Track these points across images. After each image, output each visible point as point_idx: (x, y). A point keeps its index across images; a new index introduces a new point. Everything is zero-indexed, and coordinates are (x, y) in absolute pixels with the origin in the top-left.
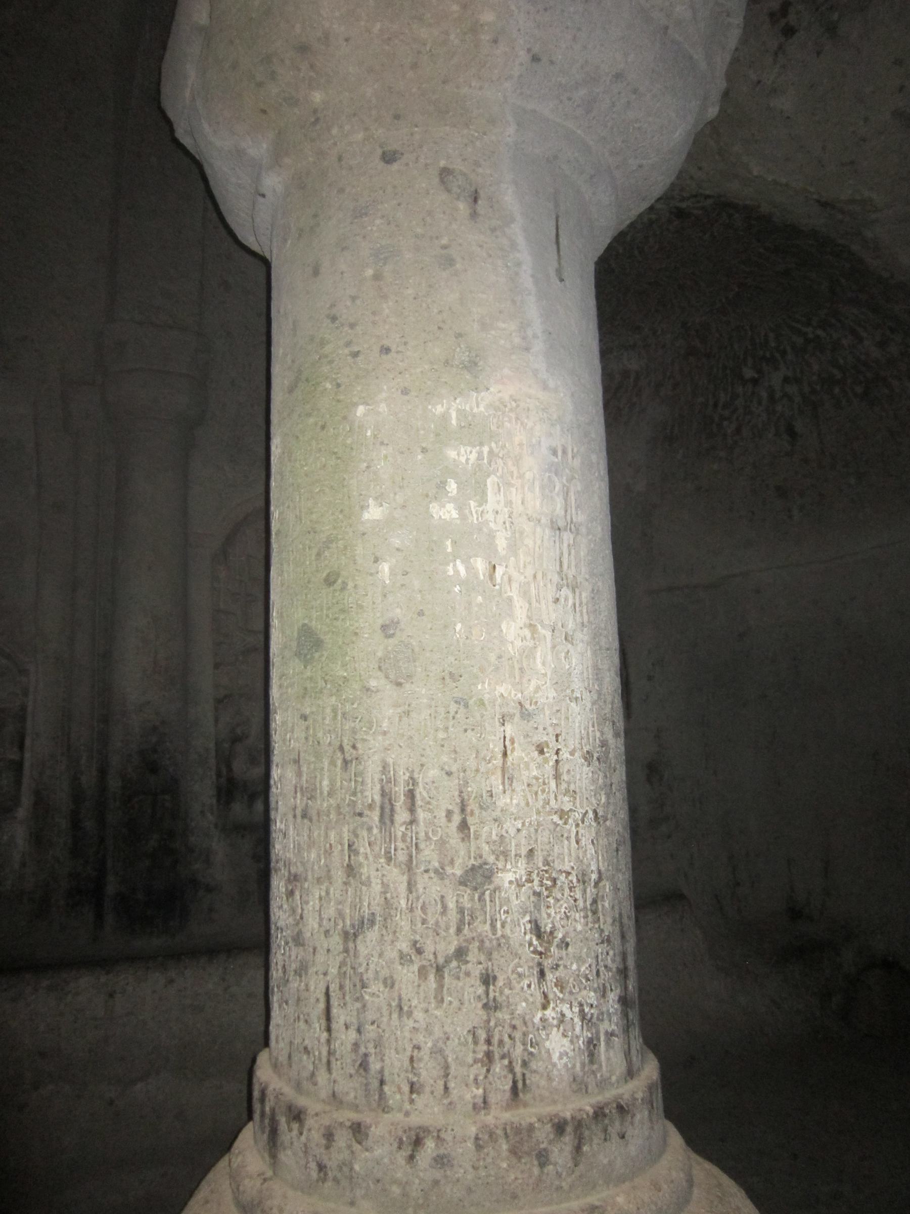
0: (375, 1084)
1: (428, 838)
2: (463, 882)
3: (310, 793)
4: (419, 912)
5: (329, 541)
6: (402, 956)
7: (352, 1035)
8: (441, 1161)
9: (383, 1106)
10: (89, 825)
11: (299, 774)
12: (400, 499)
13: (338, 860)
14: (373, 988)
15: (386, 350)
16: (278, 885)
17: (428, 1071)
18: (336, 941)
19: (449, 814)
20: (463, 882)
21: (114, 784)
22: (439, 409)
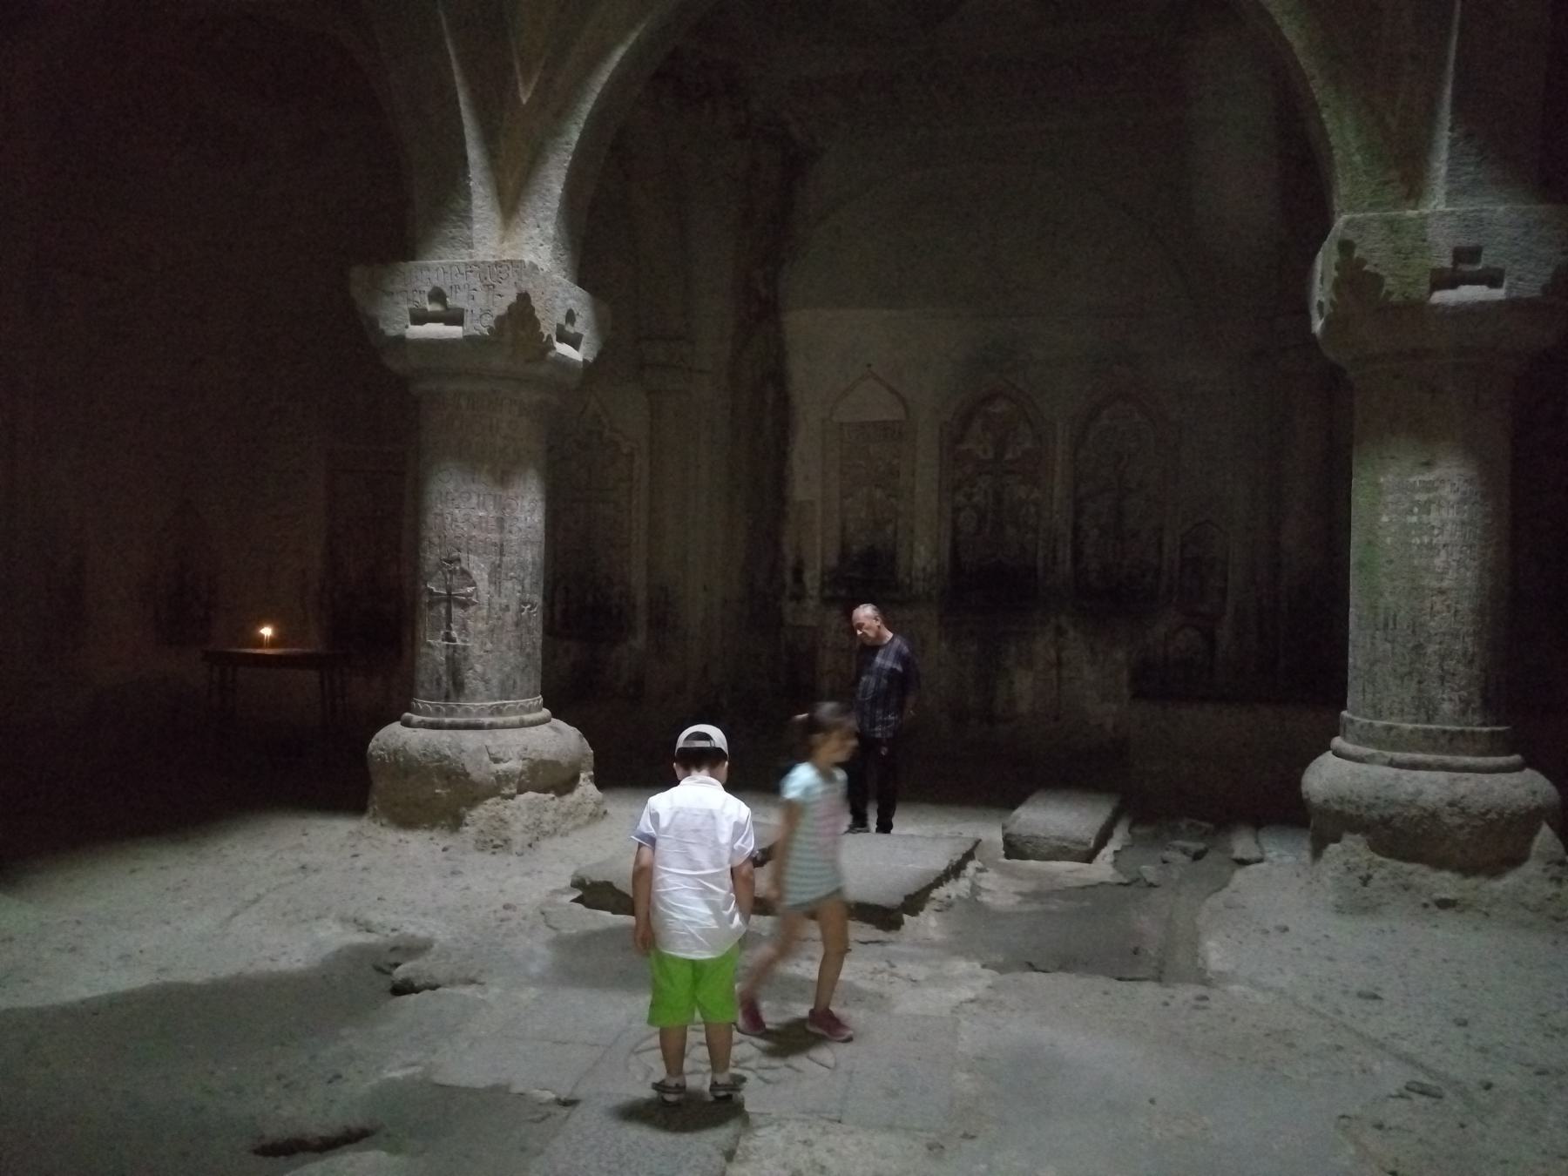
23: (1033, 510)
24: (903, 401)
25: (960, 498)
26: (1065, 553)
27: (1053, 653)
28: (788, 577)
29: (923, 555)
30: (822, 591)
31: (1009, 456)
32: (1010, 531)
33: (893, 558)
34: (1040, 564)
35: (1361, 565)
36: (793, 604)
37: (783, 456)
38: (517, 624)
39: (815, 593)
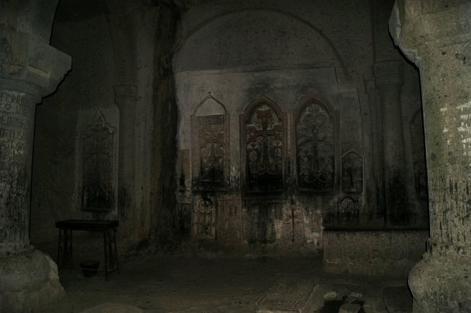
0: (450, 239)
1: (460, 194)
2: (468, 203)
3: (435, 185)
4: (458, 208)
5: (437, 136)
6: (455, 216)
7: (446, 230)
8: (464, 253)
9: (452, 244)
10: (381, 197)
11: (433, 182)
12: (451, 127)
13: (442, 198)
14: (449, 222)
15: (446, 96)
16: (430, 204)
17: (461, 237)
18: (442, 213)
19: (464, 190)
20: (468, 203)
21: (387, 186)
22: (459, 108)
23: (279, 150)
24: (225, 108)
25: (249, 147)
26: (294, 167)
27: (290, 212)
28: (178, 183)
29: (234, 171)
30: (192, 187)
31: (269, 129)
32: (271, 161)
33: (222, 172)
34: (283, 172)
35: (434, 157)
36: (180, 194)
37: (175, 132)
38: (7, 204)
39: (189, 189)
